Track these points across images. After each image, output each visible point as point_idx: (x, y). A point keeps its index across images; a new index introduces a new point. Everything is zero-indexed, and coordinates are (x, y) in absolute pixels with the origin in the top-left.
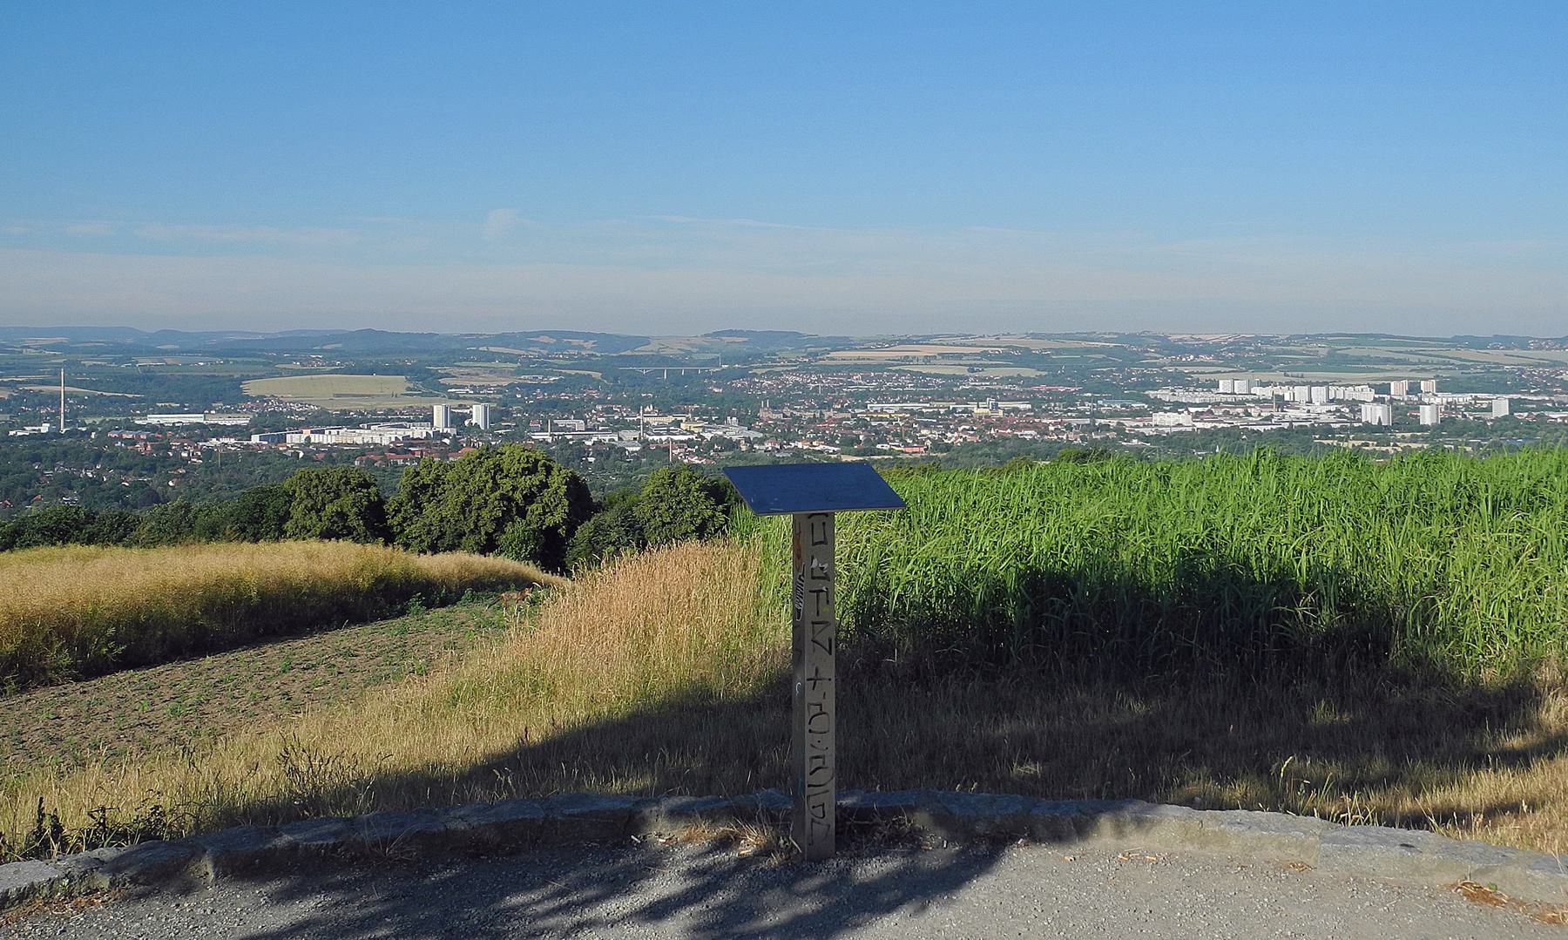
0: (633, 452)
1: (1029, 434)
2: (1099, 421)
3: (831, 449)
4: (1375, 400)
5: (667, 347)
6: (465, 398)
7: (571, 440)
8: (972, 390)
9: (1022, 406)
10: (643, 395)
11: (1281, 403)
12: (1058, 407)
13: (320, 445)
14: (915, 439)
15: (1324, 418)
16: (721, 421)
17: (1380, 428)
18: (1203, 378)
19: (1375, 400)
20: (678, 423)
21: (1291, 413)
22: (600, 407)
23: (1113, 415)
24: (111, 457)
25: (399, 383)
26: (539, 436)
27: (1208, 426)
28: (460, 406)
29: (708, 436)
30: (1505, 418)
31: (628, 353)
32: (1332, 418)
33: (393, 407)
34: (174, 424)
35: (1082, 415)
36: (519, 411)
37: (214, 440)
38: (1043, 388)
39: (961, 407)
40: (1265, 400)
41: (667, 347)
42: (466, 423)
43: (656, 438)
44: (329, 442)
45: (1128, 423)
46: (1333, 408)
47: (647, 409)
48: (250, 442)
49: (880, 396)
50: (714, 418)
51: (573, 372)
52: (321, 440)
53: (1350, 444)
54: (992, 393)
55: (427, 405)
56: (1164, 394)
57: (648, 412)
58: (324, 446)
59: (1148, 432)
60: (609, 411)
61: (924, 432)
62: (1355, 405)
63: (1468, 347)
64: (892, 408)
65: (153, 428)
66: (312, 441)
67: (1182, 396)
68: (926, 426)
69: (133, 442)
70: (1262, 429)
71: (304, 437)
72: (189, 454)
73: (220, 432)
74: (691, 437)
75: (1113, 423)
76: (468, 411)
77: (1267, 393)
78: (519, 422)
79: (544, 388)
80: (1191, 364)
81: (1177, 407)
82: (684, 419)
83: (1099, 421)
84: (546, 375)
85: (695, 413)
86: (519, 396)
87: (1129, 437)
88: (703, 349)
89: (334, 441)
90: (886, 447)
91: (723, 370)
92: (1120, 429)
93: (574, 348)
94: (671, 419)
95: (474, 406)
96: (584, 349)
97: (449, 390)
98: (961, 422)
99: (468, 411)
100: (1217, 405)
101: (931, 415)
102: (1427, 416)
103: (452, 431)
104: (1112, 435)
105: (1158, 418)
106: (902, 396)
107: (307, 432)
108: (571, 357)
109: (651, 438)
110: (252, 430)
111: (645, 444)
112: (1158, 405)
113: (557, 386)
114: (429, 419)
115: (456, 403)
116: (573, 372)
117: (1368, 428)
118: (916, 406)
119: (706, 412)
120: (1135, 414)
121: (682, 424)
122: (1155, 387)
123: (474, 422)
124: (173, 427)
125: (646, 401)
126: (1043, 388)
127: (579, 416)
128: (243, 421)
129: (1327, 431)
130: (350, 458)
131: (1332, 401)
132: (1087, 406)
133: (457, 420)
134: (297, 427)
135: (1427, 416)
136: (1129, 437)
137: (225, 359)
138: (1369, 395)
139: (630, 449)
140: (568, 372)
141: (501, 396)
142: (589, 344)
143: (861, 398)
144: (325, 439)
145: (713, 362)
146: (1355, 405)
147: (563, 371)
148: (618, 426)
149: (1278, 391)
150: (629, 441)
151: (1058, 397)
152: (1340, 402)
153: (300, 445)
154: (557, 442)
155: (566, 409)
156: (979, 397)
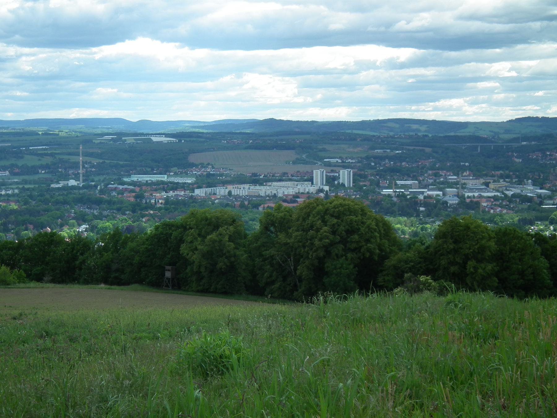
0: (453, 204)
5: (481, 129)
6: (335, 166)
7: (408, 195)
10: (462, 164)
13: (237, 197)
16: (520, 182)
20: (487, 184)
22: (430, 172)
24: (110, 202)
25: (291, 155)
26: (386, 191)
28: (332, 171)
29: (510, 193)
31: (452, 134)
33: (285, 171)
34: (147, 181)
36: (372, 175)
37: (171, 192)
41: (481, 129)
42: (336, 182)
43: (470, 194)
44: (244, 194)
47: (465, 174)
48: (193, 194)
50: (514, 180)
51: (411, 148)
52: (238, 193)
55: (310, 171)
57: (465, 176)
58: (240, 197)
65: (133, 183)
66: (233, 194)
69: (122, 192)
71: (227, 191)
72: (155, 201)
73: (175, 187)
74: (496, 194)
76: (337, 174)
78: (371, 182)
79: (390, 158)
82: (491, 181)
84: (392, 149)
85: (501, 177)
86: (373, 164)
88: (507, 131)
89: (246, 194)
91: (523, 146)
93: (414, 130)
94: (482, 181)
95: (341, 171)
96: (419, 131)
97: (325, 160)
99: (337, 174)
103: (326, 188)
107: (230, 187)
108: (411, 137)
109: (466, 195)
110: (195, 186)
113: (399, 158)
114: (311, 180)
115: (330, 169)
116: (411, 148)
119: (508, 177)
121: (490, 185)
123: (341, 181)
124: (147, 184)
125: (464, 169)
127: (414, 178)
128: (189, 181)
133: (331, 181)
134: (224, 183)
137: (179, 139)
139: (450, 202)
140: (407, 147)
141: (360, 164)
142: (423, 128)
144: (241, 192)
145: (516, 140)
147: (405, 147)
148: (442, 186)
153: (225, 196)
154: (398, 196)
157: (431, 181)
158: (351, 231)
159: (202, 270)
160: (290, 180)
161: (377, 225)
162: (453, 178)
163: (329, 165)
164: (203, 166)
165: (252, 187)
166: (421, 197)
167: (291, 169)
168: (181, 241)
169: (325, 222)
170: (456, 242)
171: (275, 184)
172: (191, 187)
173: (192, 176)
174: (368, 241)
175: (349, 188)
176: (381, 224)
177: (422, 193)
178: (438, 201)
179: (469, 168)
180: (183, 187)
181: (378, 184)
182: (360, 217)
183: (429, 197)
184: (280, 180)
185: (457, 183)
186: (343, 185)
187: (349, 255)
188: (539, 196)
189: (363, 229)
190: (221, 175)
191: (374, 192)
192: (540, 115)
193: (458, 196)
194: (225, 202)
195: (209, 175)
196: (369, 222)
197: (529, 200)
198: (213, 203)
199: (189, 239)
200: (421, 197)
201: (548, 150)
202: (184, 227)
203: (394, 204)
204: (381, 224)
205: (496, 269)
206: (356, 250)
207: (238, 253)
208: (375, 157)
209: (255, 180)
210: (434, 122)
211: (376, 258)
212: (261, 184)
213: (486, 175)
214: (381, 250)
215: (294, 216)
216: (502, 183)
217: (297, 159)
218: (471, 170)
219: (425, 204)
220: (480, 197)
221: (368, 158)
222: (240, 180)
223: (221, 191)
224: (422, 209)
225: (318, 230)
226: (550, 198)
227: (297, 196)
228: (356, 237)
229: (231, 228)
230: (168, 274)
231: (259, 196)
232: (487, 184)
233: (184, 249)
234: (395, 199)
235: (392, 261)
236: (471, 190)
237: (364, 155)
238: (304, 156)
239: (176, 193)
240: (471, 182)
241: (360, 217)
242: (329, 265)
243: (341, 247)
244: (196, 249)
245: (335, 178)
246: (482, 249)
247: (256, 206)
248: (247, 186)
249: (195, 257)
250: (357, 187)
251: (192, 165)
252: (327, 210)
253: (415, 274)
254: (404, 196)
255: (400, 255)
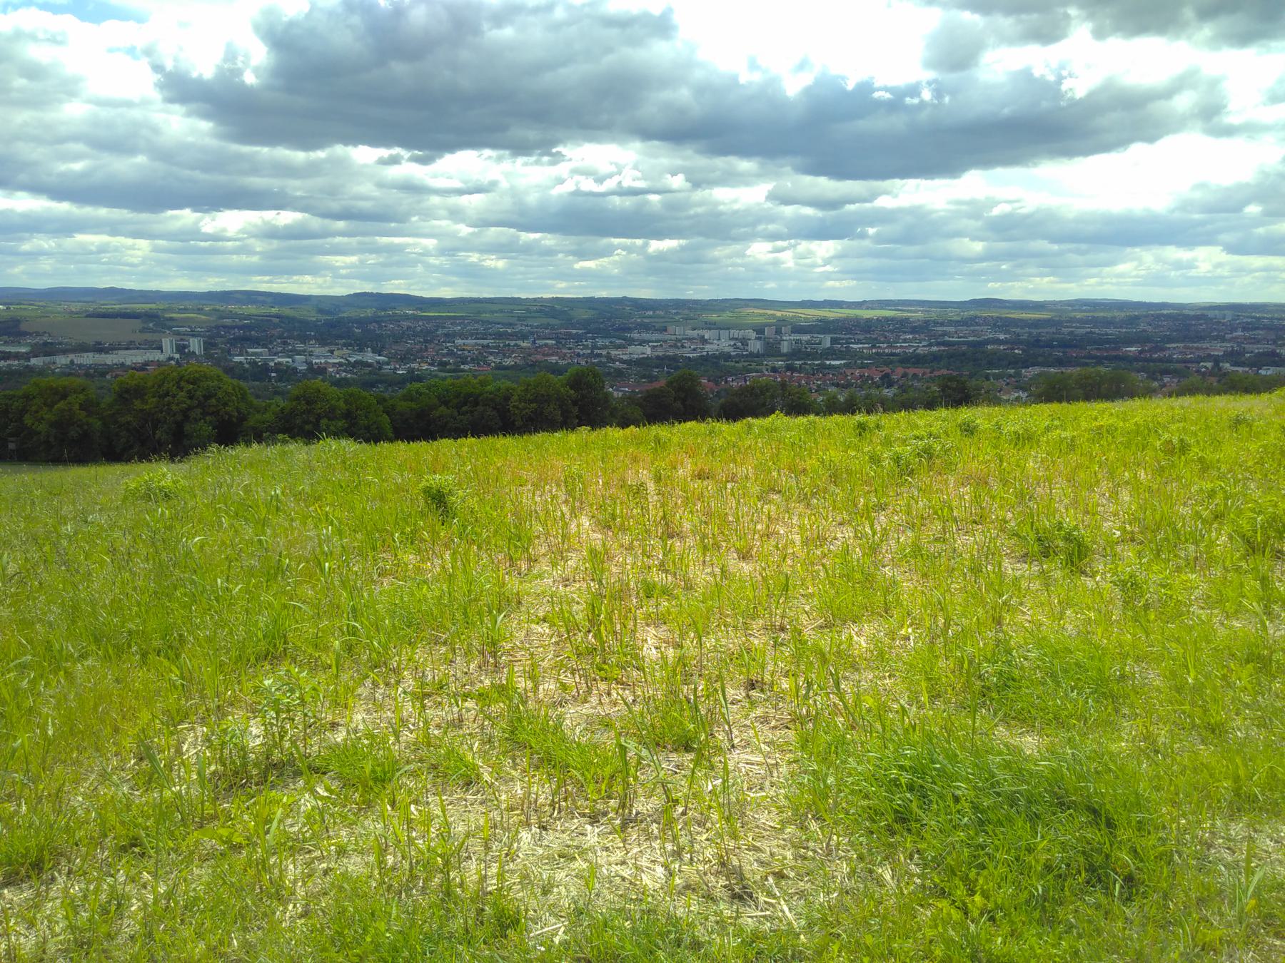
1: (554, 359)
2: (596, 351)
3: (433, 368)
4: (756, 338)
8: (520, 331)
9: (550, 342)
11: (703, 341)
12: (571, 343)
13: (80, 366)
14: (485, 363)
15: (727, 349)
16: (361, 350)
17: (758, 355)
18: (658, 326)
19: (756, 338)
20: (332, 352)
21: (708, 347)
23: (605, 347)
25: (137, 324)
26: (237, 359)
27: (661, 354)
28: (182, 340)
29: (352, 360)
30: (828, 348)
32: (732, 349)
35: (586, 347)
38: (563, 331)
39: (512, 343)
40: (694, 339)
43: (317, 361)
45: (613, 352)
46: (732, 343)
49: (463, 336)
53: (740, 365)
54: (532, 333)
56: (635, 335)
59: (625, 357)
60: (285, 343)
61: (491, 358)
62: (744, 341)
63: (809, 308)
64: (470, 342)
67: (646, 336)
68: (491, 354)
70: (691, 355)
71: (69, 359)
75: (604, 352)
77: (695, 333)
78: (223, 350)
79: (240, 328)
80: (650, 317)
81: (642, 342)
83: (596, 351)
85: (344, 345)
87: (614, 361)
90: (467, 367)
92: (608, 357)
94: (327, 348)
98: (513, 352)
100: (665, 341)
101: (494, 347)
102: (785, 348)
103: (177, 356)
104: (604, 360)
105: (631, 349)
106: (475, 335)
107: (71, 356)
111: (310, 364)
112: (631, 342)
114: (160, 348)
115: (178, 337)
117: (751, 355)
118: (485, 342)
119: (350, 345)
120: (618, 347)
122: (629, 330)
125: (310, 338)
126: (563, 331)
127: (264, 346)
128: (23, 350)
129: (727, 357)
130: (103, 374)
131: (730, 339)
132: (589, 343)
133: (181, 349)
134: (65, 352)
135: (785, 348)
136: (614, 361)
138: (753, 335)
143: (450, 336)
146: (744, 341)
149: (701, 332)
150: (300, 363)
151: (570, 336)
152: (736, 339)
155: (256, 342)
156: (524, 337)
157: (280, 349)
158: (207, 397)
159: (52, 439)
160: (138, 348)
161: (234, 389)
162: (300, 346)
163: (178, 333)
164: (38, 334)
165: (97, 356)
166: (272, 364)
167: (139, 338)
168: (23, 411)
169: (181, 389)
170: (308, 403)
171: (120, 352)
172: (27, 357)
173: (27, 344)
174: (225, 404)
175: (201, 356)
176: (237, 389)
177: (273, 360)
178: (288, 367)
179: (315, 337)
180: (17, 356)
181: (229, 351)
182: (216, 382)
183: (279, 363)
184: (127, 349)
185: (305, 351)
186: (194, 353)
187: (208, 418)
188: (378, 362)
189: (220, 394)
190: (60, 343)
191: (226, 360)
192: (375, 291)
193: (306, 362)
194: (68, 370)
195: (45, 344)
196: (225, 387)
197: (370, 365)
198: (53, 373)
199: (34, 408)
200: (272, 364)
201: (382, 321)
202: (27, 397)
203: (246, 370)
204: (237, 389)
205: (346, 425)
206: (216, 413)
207: (91, 420)
208: (225, 327)
209: (99, 348)
210: (279, 295)
211: (234, 420)
212: (107, 353)
213: (331, 344)
214: (239, 413)
215: (150, 384)
216: (346, 351)
217: (144, 328)
218: (317, 340)
219: (276, 371)
220: (326, 363)
221: (217, 327)
222: (83, 348)
223: (62, 360)
224: (273, 374)
225: (174, 396)
226: (388, 364)
227: (147, 364)
228: (213, 401)
229: (82, 397)
230: (11, 446)
231: (106, 364)
232: (332, 352)
233: (28, 420)
234: (247, 366)
235: (251, 422)
236: (318, 357)
237: (213, 325)
238: (151, 325)
239: (9, 362)
240: (318, 350)
241: (216, 382)
242: (188, 428)
243: (199, 411)
244: (42, 418)
245: (185, 347)
246: (333, 409)
247: (103, 374)
248: (91, 355)
249: (42, 427)
250: (208, 356)
251: (25, 334)
252: (183, 376)
253: (273, 433)
254: (255, 363)
255: (258, 416)
